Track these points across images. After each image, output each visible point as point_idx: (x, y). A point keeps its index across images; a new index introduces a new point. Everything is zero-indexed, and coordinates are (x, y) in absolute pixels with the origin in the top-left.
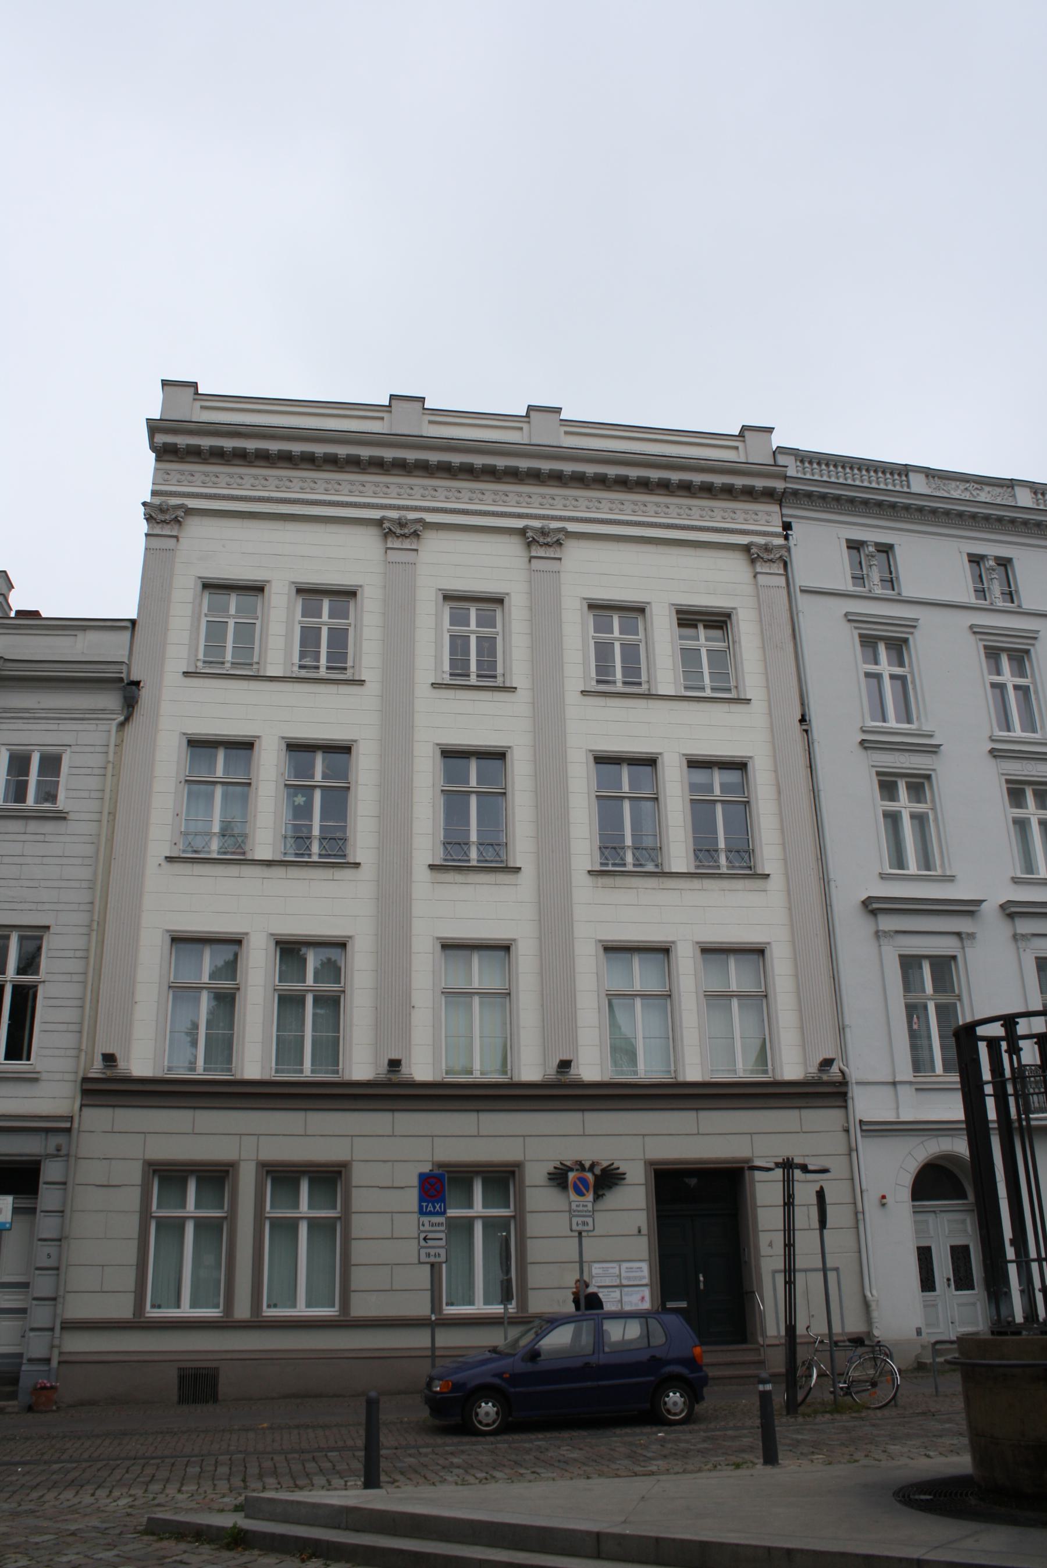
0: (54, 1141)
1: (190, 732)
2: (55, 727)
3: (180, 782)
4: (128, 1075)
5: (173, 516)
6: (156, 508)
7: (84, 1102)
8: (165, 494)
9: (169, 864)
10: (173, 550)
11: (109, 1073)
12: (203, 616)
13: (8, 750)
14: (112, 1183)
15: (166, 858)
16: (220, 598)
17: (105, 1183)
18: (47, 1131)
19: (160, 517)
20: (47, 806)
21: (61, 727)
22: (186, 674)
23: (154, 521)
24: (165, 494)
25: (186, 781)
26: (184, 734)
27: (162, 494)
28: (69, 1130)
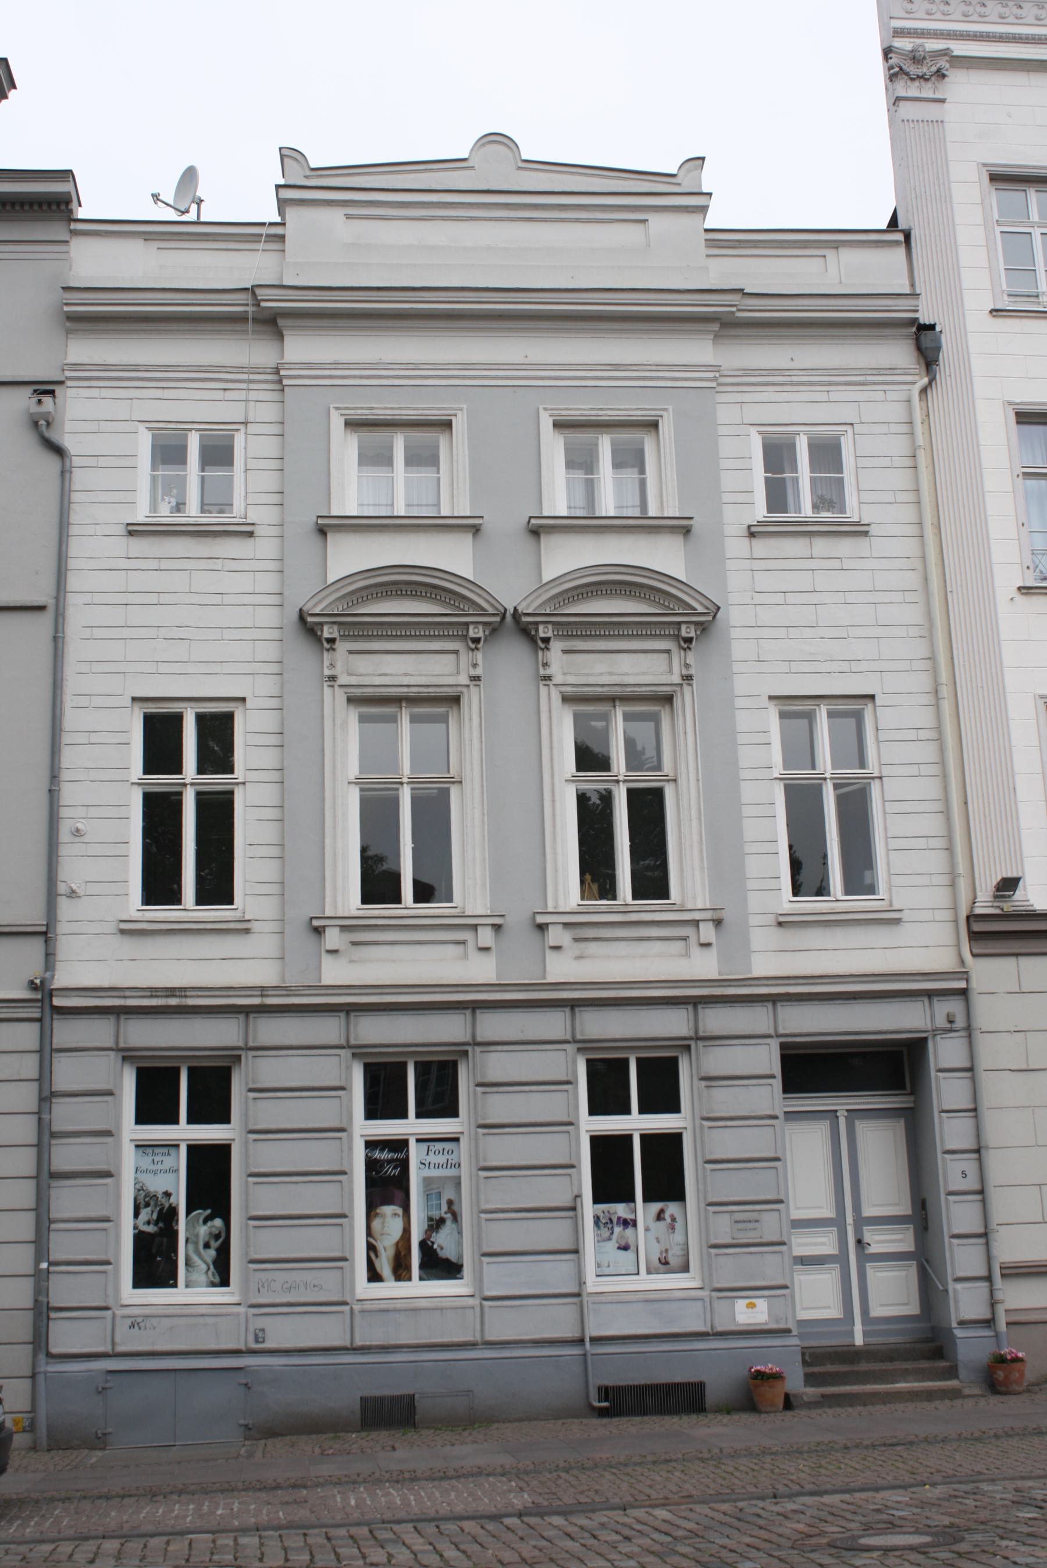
0: (944, 1008)
1: (1018, 400)
2: (823, 397)
3: (1018, 476)
4: (1030, 908)
5: (934, 69)
6: (906, 55)
7: (975, 951)
8: (915, 33)
9: (1024, 598)
10: (942, 122)
11: (1008, 907)
12: (996, 225)
13: (760, 433)
14: (1032, 1067)
15: (1019, 589)
16: (1014, 196)
17: (1024, 1067)
18: (930, 994)
19: (913, 70)
20: (826, 515)
21: (833, 396)
22: (995, 312)
23: (906, 77)
24: (915, 33)
25: (1024, 474)
26: (1010, 403)
27: (909, 33)
28: (964, 993)
